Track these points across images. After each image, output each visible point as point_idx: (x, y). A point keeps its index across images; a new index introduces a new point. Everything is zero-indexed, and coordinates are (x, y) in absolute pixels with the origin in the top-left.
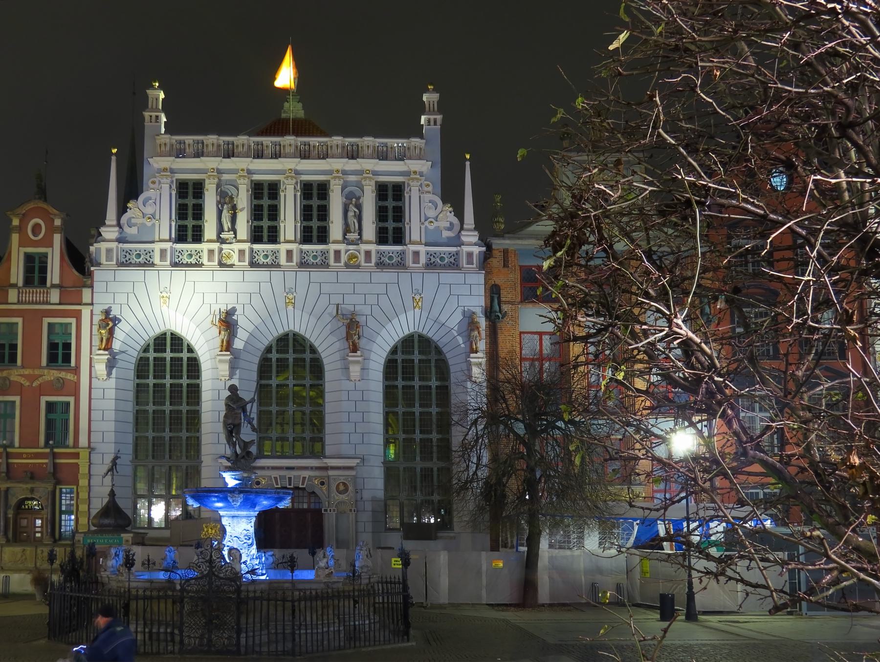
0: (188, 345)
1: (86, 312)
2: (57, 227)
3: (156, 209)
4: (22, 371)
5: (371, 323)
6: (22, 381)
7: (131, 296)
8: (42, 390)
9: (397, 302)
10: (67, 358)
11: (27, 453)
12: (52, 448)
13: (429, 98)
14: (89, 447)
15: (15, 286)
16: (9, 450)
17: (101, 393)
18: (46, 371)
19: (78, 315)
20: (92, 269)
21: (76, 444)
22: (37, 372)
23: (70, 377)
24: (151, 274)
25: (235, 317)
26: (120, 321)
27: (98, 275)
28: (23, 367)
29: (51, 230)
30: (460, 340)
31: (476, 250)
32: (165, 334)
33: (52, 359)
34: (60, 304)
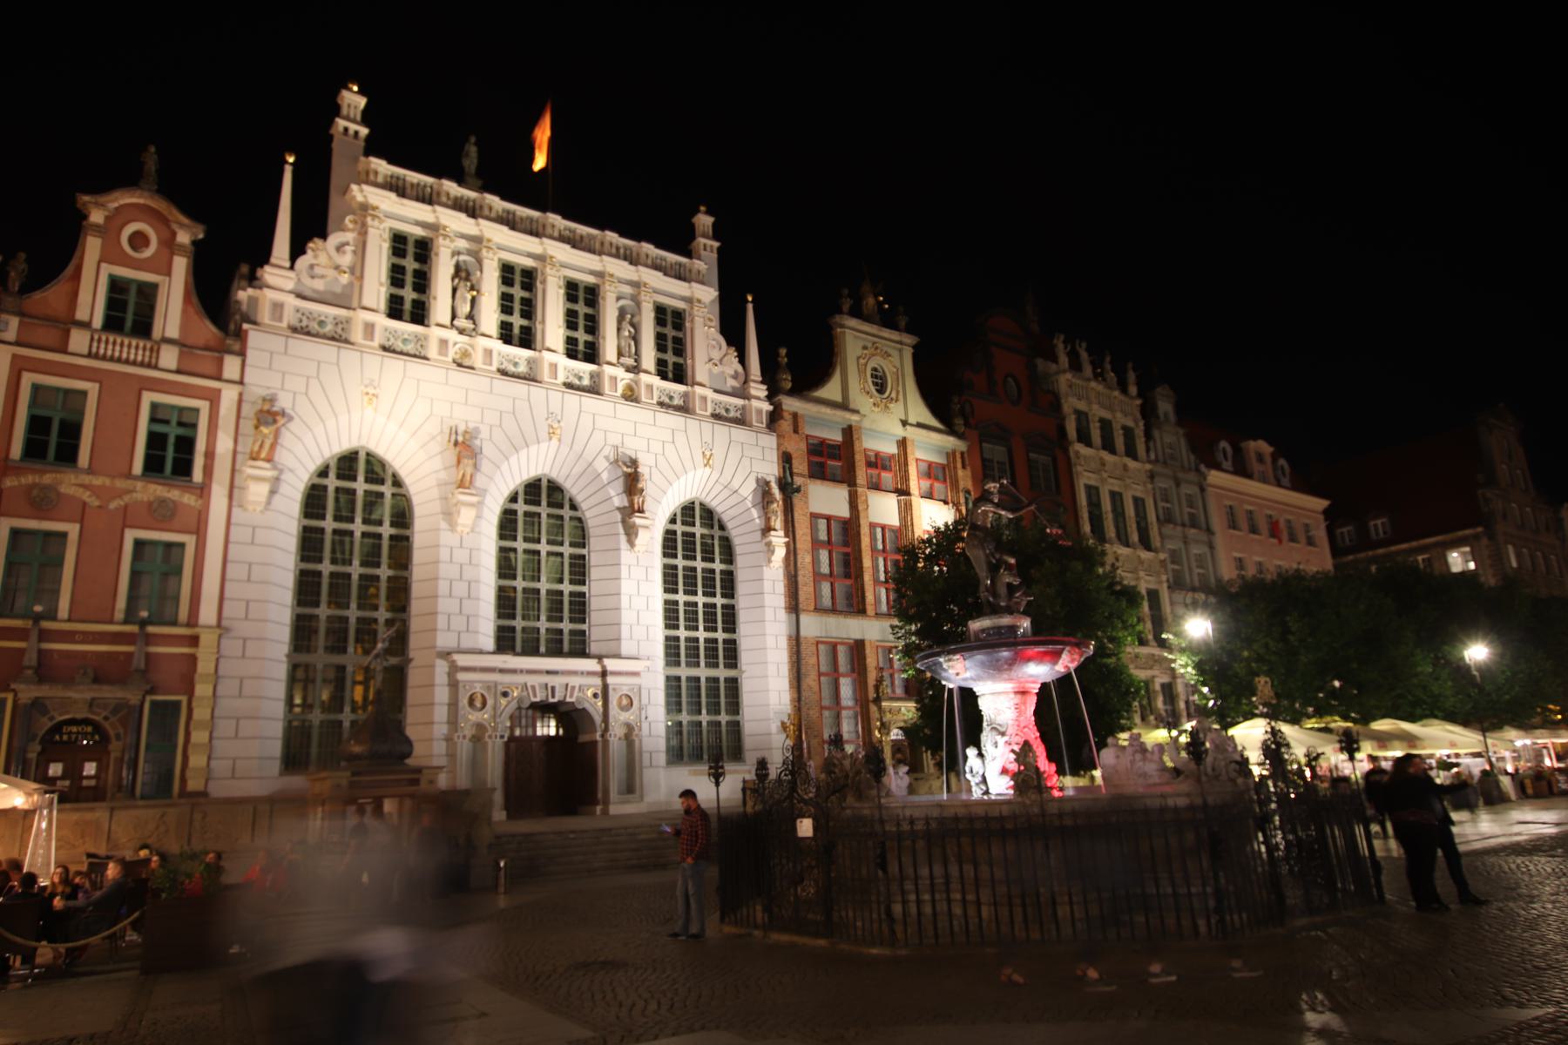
0: (394, 476)
1: (229, 395)
2: (181, 246)
3: (354, 258)
4: (87, 479)
5: (656, 477)
6: (86, 496)
7: (314, 382)
8: (127, 518)
9: (686, 455)
10: (183, 468)
11: (83, 633)
12: (143, 623)
13: (704, 221)
14: (219, 625)
15: (86, 325)
16: (46, 624)
17: (251, 536)
18: (139, 485)
19: (214, 398)
20: (245, 326)
21: (193, 621)
22: (121, 484)
23: (189, 499)
24: (348, 355)
25: (477, 442)
26: (291, 419)
27: (255, 338)
28: (91, 471)
29: (169, 244)
30: (755, 513)
31: (767, 407)
32: (356, 453)
33: (153, 466)
34: (178, 372)
